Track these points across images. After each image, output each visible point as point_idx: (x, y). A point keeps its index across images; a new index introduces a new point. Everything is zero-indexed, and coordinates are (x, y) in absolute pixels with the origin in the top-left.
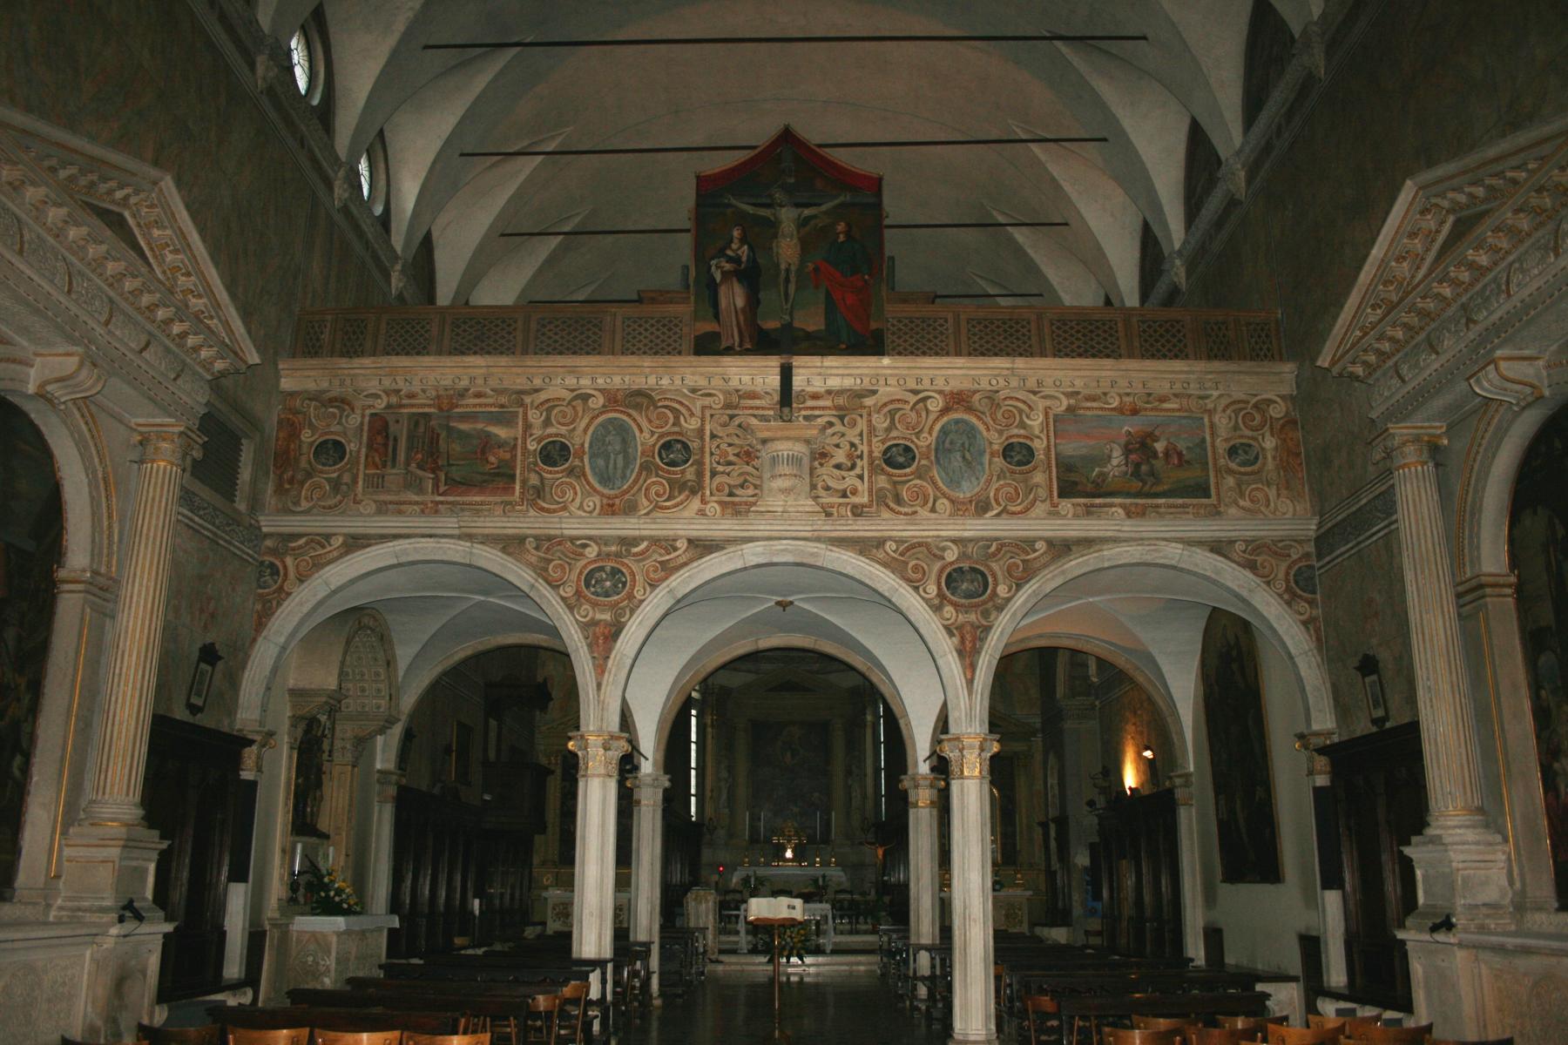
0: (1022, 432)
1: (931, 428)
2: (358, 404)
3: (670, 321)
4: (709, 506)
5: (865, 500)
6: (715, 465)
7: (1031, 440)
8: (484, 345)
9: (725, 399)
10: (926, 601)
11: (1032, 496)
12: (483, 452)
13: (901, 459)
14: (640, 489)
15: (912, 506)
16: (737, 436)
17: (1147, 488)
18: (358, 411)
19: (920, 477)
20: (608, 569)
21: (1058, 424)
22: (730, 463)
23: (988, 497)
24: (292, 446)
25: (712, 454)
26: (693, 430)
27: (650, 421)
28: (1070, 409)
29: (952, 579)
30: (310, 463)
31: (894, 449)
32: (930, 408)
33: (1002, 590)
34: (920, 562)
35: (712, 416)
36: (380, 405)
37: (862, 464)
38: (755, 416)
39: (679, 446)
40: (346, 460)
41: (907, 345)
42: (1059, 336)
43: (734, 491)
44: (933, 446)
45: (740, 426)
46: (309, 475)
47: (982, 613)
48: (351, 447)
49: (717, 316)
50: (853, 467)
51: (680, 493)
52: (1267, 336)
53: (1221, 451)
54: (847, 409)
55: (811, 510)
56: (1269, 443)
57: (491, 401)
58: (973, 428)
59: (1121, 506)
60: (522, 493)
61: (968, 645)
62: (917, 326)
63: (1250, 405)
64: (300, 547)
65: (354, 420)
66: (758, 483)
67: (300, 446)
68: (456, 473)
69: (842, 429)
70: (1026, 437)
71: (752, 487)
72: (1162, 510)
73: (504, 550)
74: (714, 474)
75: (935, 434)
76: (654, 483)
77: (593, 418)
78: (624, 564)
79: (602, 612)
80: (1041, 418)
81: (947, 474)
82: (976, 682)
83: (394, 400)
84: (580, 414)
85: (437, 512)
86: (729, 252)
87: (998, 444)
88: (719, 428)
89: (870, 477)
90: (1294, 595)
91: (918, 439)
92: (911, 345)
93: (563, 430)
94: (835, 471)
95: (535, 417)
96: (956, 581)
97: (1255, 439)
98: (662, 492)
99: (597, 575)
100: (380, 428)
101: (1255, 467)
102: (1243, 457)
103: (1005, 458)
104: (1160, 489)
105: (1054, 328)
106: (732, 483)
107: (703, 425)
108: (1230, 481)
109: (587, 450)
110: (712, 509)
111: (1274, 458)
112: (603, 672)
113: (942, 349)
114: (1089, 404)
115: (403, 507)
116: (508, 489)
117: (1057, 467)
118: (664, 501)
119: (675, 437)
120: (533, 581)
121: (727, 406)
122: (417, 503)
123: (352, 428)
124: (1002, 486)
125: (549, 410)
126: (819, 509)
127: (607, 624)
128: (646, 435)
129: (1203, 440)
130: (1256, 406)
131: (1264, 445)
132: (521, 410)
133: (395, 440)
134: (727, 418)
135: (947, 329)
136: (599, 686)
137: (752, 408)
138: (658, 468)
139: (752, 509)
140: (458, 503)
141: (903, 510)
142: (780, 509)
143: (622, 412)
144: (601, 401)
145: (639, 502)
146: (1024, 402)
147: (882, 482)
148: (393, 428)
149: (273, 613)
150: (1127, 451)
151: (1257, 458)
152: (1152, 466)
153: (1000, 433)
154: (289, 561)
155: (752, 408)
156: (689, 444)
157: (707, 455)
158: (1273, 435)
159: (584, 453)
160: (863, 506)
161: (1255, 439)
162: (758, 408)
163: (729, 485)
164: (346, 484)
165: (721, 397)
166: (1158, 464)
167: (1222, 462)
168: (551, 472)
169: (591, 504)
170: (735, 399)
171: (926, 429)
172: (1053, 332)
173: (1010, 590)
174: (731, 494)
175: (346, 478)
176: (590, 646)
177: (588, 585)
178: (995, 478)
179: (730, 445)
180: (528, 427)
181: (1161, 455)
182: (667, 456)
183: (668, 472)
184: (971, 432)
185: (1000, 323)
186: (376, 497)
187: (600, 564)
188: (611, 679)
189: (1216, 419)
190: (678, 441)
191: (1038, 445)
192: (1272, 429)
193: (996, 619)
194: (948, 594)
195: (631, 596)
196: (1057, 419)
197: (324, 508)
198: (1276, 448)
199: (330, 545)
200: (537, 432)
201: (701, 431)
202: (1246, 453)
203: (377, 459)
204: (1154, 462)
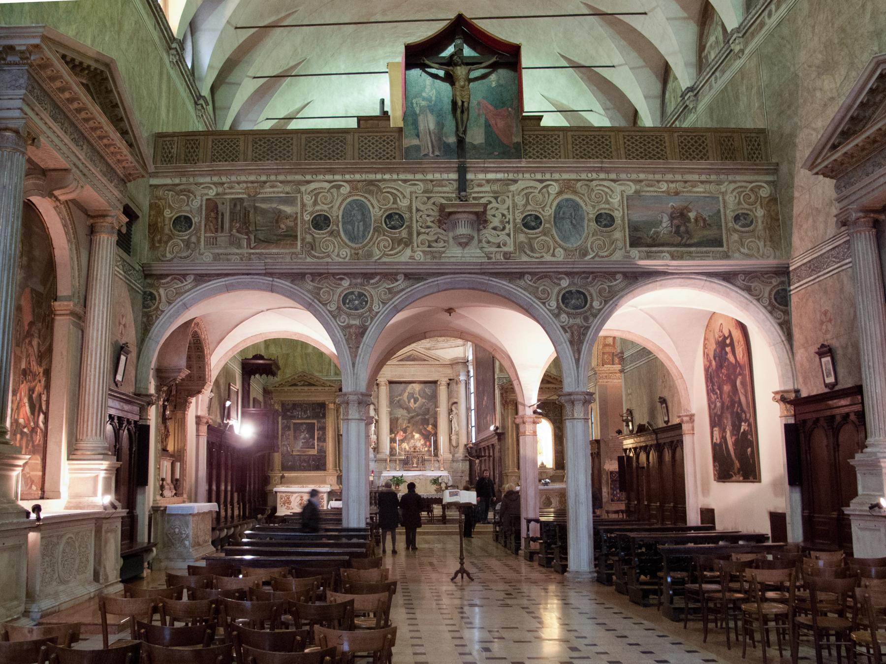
0: (607, 206)
1: (551, 204)
2: (198, 193)
3: (388, 138)
5: (512, 249)
6: (419, 228)
7: (613, 211)
8: (273, 154)
9: (424, 187)
10: (550, 311)
11: (613, 246)
12: (277, 222)
13: (533, 224)
14: (374, 243)
17: (684, 241)
18: (199, 198)
19: (545, 235)
20: (356, 293)
21: (630, 201)
22: (428, 227)
23: (587, 247)
24: (159, 220)
25: (417, 221)
27: (379, 201)
28: (636, 192)
29: (566, 298)
30: (171, 231)
32: (550, 191)
33: (596, 304)
34: (546, 287)
35: (417, 197)
36: (212, 193)
37: (510, 227)
38: (443, 197)
39: (397, 217)
40: (193, 228)
41: (534, 152)
42: (629, 145)
43: (433, 245)
44: (553, 216)
45: (434, 204)
46: (170, 238)
47: (584, 318)
48: (195, 220)
49: (418, 136)
50: (504, 228)
52: (758, 145)
53: (730, 218)
56: (760, 213)
57: (280, 190)
58: (578, 204)
59: (668, 252)
60: (302, 247)
61: (576, 338)
62: (541, 140)
63: (748, 189)
64: (168, 283)
65: (196, 203)
66: (446, 239)
67: (164, 220)
68: (261, 236)
69: (497, 205)
70: (610, 210)
71: (442, 242)
72: (694, 255)
73: (292, 282)
74: (419, 234)
75: (554, 208)
76: (382, 240)
77: (344, 200)
78: (365, 290)
79: (354, 319)
80: (619, 198)
81: (561, 233)
82: (581, 360)
83: (220, 190)
84: (335, 198)
85: (250, 259)
86: (424, 94)
87: (592, 216)
89: (514, 235)
90: (773, 307)
91: (543, 211)
92: (538, 152)
93: (325, 207)
95: (308, 200)
96: (568, 299)
97: (751, 210)
98: (387, 245)
99: (350, 297)
100: (212, 207)
101: (751, 228)
102: (743, 222)
103: (597, 223)
104: (692, 241)
105: (625, 140)
106: (430, 239)
108: (735, 237)
109: (340, 219)
111: (763, 222)
112: (356, 356)
113: (557, 154)
114: (648, 189)
115: (229, 257)
116: (294, 245)
117: (629, 228)
118: (390, 250)
119: (394, 211)
120: (311, 301)
121: (425, 192)
122: (237, 254)
123: (194, 207)
124: (596, 240)
125: (316, 195)
126: (483, 255)
127: (356, 327)
128: (377, 210)
129: (719, 211)
130: (752, 190)
131: (756, 214)
132: (299, 195)
133: (223, 215)
134: (426, 199)
136: (354, 364)
137: (441, 192)
138: (384, 230)
140: (262, 254)
142: (460, 255)
143: (361, 196)
144: (348, 189)
145: (374, 252)
146: (608, 188)
147: (522, 238)
148: (220, 207)
149: (153, 324)
150: (672, 218)
151: (752, 222)
152: (687, 227)
153: (594, 207)
154: (162, 291)
155: (441, 192)
158: (762, 208)
159: (339, 221)
160: (510, 253)
161: (751, 210)
162: (444, 192)
164: (194, 243)
165: (422, 186)
166: (691, 226)
167: (730, 225)
168: (319, 234)
169: (344, 253)
170: (430, 187)
171: (548, 205)
172: (625, 143)
173: (601, 303)
174: (429, 246)
175: (194, 239)
176: (347, 340)
177: (344, 304)
178: (591, 235)
179: (428, 216)
180: (303, 205)
181: (693, 220)
183: (391, 233)
184: (576, 207)
185: (592, 138)
186: (212, 251)
187: (351, 290)
188: (361, 361)
189: (727, 198)
190: (396, 214)
191: (617, 215)
192: (761, 204)
193: (593, 321)
194: (563, 307)
195: (371, 310)
196: (628, 198)
197: (181, 258)
198: (764, 216)
199: (186, 281)
200: (310, 209)
201: (410, 208)
202: (745, 219)
203: (212, 227)
204: (688, 224)
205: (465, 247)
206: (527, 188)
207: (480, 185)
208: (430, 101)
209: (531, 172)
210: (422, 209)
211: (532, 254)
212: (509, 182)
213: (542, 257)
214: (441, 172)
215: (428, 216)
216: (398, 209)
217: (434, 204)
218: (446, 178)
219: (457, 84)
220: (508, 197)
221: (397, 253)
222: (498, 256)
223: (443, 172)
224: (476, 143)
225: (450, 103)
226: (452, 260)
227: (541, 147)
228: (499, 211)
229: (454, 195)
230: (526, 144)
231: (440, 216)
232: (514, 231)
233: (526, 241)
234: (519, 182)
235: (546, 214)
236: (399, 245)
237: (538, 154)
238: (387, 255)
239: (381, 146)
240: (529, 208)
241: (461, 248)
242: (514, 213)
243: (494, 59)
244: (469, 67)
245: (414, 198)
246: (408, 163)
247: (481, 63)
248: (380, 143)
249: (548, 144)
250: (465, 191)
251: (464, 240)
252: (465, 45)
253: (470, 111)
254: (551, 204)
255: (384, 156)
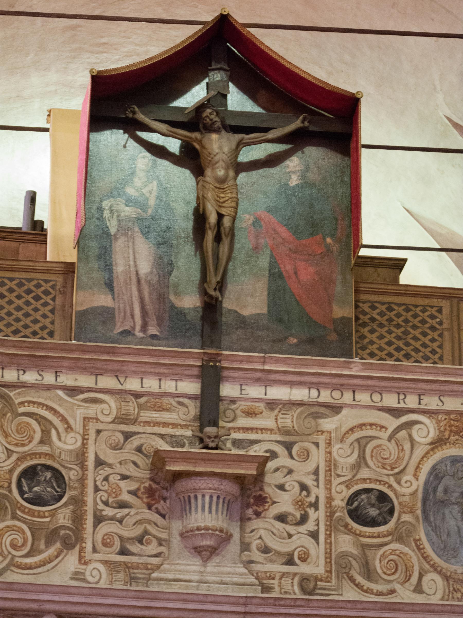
1: (418, 468)
3: (38, 286)
4: (90, 567)
5: (320, 570)
6: (101, 506)
13: (373, 512)
15: (390, 582)
16: (135, 464)
19: (400, 539)
22: (123, 505)
25: (97, 489)
26: (70, 451)
31: (363, 496)
35: (98, 432)
38: (162, 436)
39: (48, 475)
44: (420, 495)
45: (139, 449)
49: (110, 285)
50: (304, 519)
51: (48, 545)
54: (297, 434)
55: (242, 580)
62: (398, 315)
66: (164, 536)
69: (289, 463)
71: (155, 543)
81: (439, 536)
86: (130, 191)
88: (109, 451)
89: (328, 536)
91: (399, 483)
92: (390, 343)
94: (279, 525)
106: (126, 534)
107: (84, 445)
110: (95, 573)
113: (434, 352)
118: (26, 556)
119: (42, 461)
121: (121, 419)
126: (252, 580)
134: (121, 437)
135: (441, 323)
137: (157, 424)
138: (16, 505)
139: (154, 575)
141: (375, 587)
142: (195, 577)
155: (157, 424)
156: (64, 472)
157: (90, 489)
160: (317, 579)
162: (166, 425)
163: (121, 538)
165: (113, 405)
171: (411, 469)
174: (123, 552)
179: (124, 477)
182: (30, 489)
183: (31, 513)
190: (48, 468)
205: (209, 558)
206: (361, 426)
207: (251, 413)
208: (144, 208)
209: (373, 390)
210: (110, 461)
211: (367, 584)
212: (322, 410)
213: (393, 591)
214: (160, 377)
215: (124, 477)
216: (51, 456)
217: (139, 449)
218: (172, 390)
219: (208, 172)
220: (317, 445)
221: (43, 564)
222: (287, 582)
223: (165, 375)
224: (246, 312)
225: (191, 216)
226: (176, 588)
227: (399, 332)
228: (295, 476)
229: (189, 433)
230: (364, 325)
231: (152, 479)
232: (329, 528)
233: (354, 550)
234: (345, 411)
235: (405, 490)
236: (48, 544)
237: (391, 349)
238: (19, 567)
239: (20, 302)
240: (364, 473)
241: (198, 561)
242: (328, 483)
243: (296, 124)
244: (241, 136)
245: (92, 434)
246: (82, 350)
247: (266, 130)
248: (19, 297)
249: (414, 327)
250: (215, 424)
251: (208, 542)
252: (232, 87)
253: (237, 238)
254: (418, 468)
255: (26, 327)
